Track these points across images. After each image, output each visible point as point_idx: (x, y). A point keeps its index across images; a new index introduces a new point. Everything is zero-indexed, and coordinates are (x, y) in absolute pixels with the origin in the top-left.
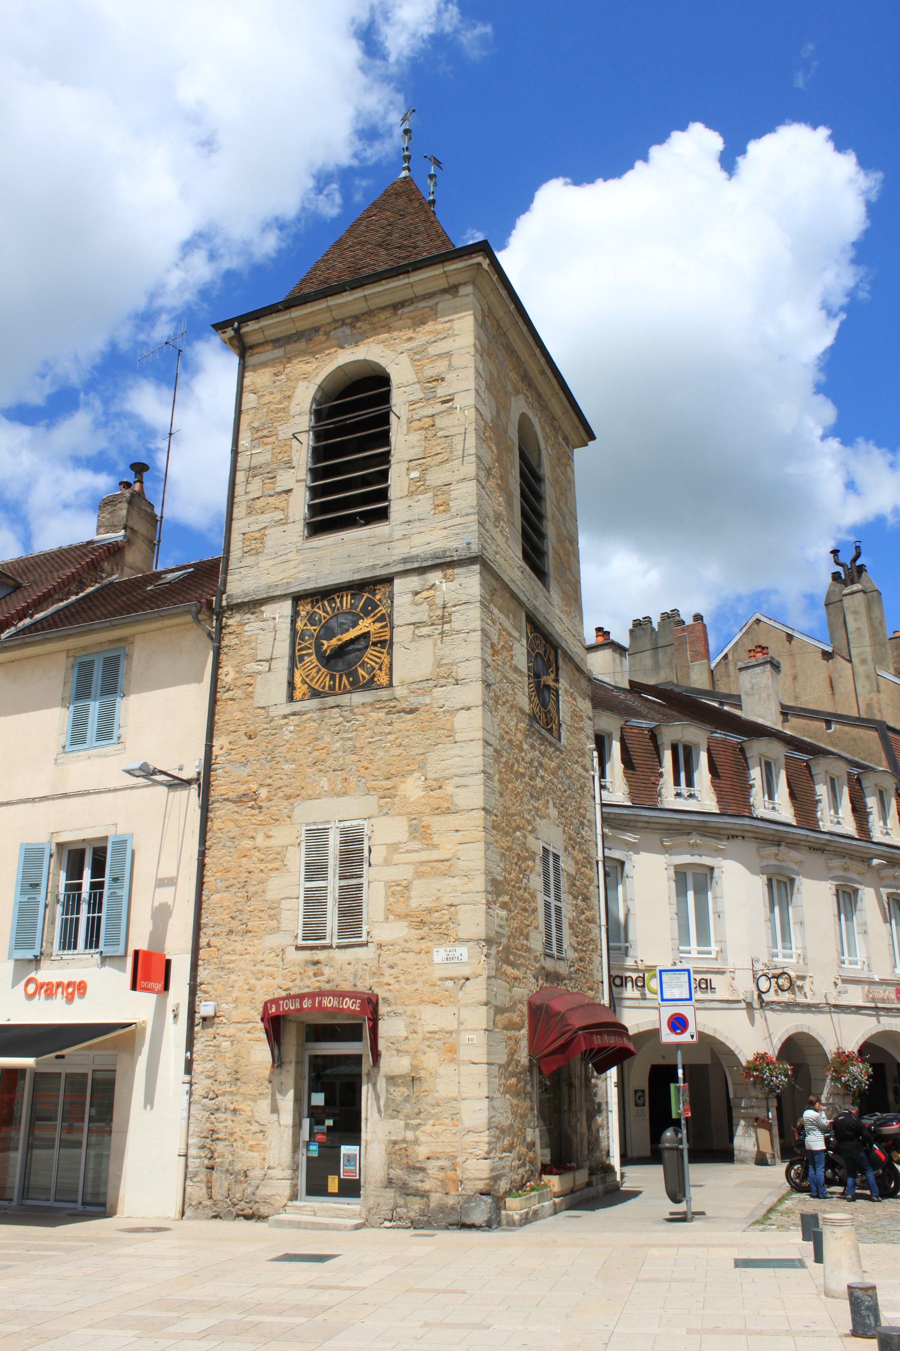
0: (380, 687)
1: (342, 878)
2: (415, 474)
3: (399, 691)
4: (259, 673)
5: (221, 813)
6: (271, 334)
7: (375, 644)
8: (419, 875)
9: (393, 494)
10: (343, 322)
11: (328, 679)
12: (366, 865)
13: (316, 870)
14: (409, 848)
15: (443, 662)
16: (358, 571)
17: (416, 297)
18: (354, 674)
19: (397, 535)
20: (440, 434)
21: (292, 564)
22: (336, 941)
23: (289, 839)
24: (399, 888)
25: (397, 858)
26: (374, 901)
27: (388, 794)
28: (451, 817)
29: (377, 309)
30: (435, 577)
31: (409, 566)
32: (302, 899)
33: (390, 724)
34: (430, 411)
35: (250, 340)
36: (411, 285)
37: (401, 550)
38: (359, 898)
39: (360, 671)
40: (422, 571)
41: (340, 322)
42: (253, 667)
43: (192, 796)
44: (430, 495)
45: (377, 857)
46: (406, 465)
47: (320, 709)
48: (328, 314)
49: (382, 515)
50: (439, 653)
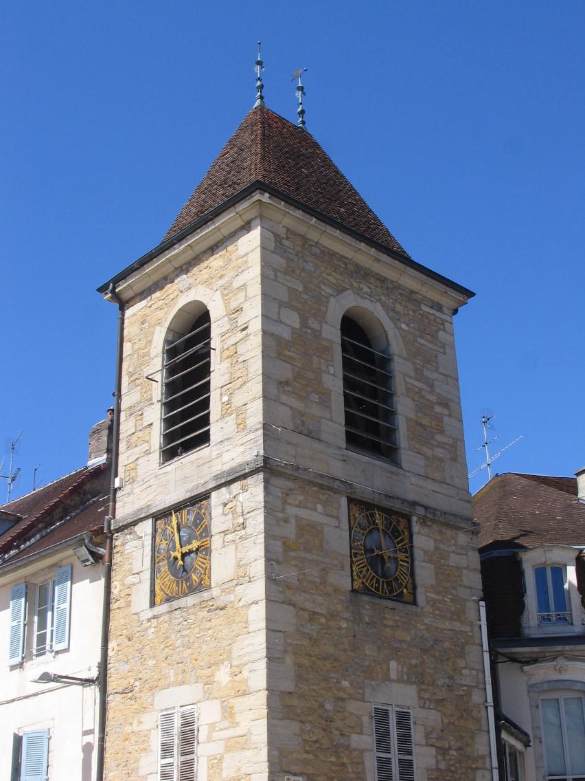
2: (225, 399)
3: (215, 592)
4: (134, 584)
5: (113, 701)
6: (138, 288)
8: (228, 749)
9: (212, 418)
11: (175, 585)
13: (166, 750)
14: (222, 727)
15: (241, 564)
17: (225, 237)
18: (189, 579)
19: (214, 455)
20: (240, 360)
23: (151, 721)
24: (216, 761)
27: (209, 682)
28: (246, 698)
29: (201, 253)
33: (210, 621)
35: (125, 296)
36: (218, 229)
38: (191, 771)
40: (229, 483)
41: (179, 269)
42: (130, 580)
43: (93, 692)
44: (234, 416)
45: (202, 736)
47: (169, 612)
48: (169, 265)
50: (239, 555)
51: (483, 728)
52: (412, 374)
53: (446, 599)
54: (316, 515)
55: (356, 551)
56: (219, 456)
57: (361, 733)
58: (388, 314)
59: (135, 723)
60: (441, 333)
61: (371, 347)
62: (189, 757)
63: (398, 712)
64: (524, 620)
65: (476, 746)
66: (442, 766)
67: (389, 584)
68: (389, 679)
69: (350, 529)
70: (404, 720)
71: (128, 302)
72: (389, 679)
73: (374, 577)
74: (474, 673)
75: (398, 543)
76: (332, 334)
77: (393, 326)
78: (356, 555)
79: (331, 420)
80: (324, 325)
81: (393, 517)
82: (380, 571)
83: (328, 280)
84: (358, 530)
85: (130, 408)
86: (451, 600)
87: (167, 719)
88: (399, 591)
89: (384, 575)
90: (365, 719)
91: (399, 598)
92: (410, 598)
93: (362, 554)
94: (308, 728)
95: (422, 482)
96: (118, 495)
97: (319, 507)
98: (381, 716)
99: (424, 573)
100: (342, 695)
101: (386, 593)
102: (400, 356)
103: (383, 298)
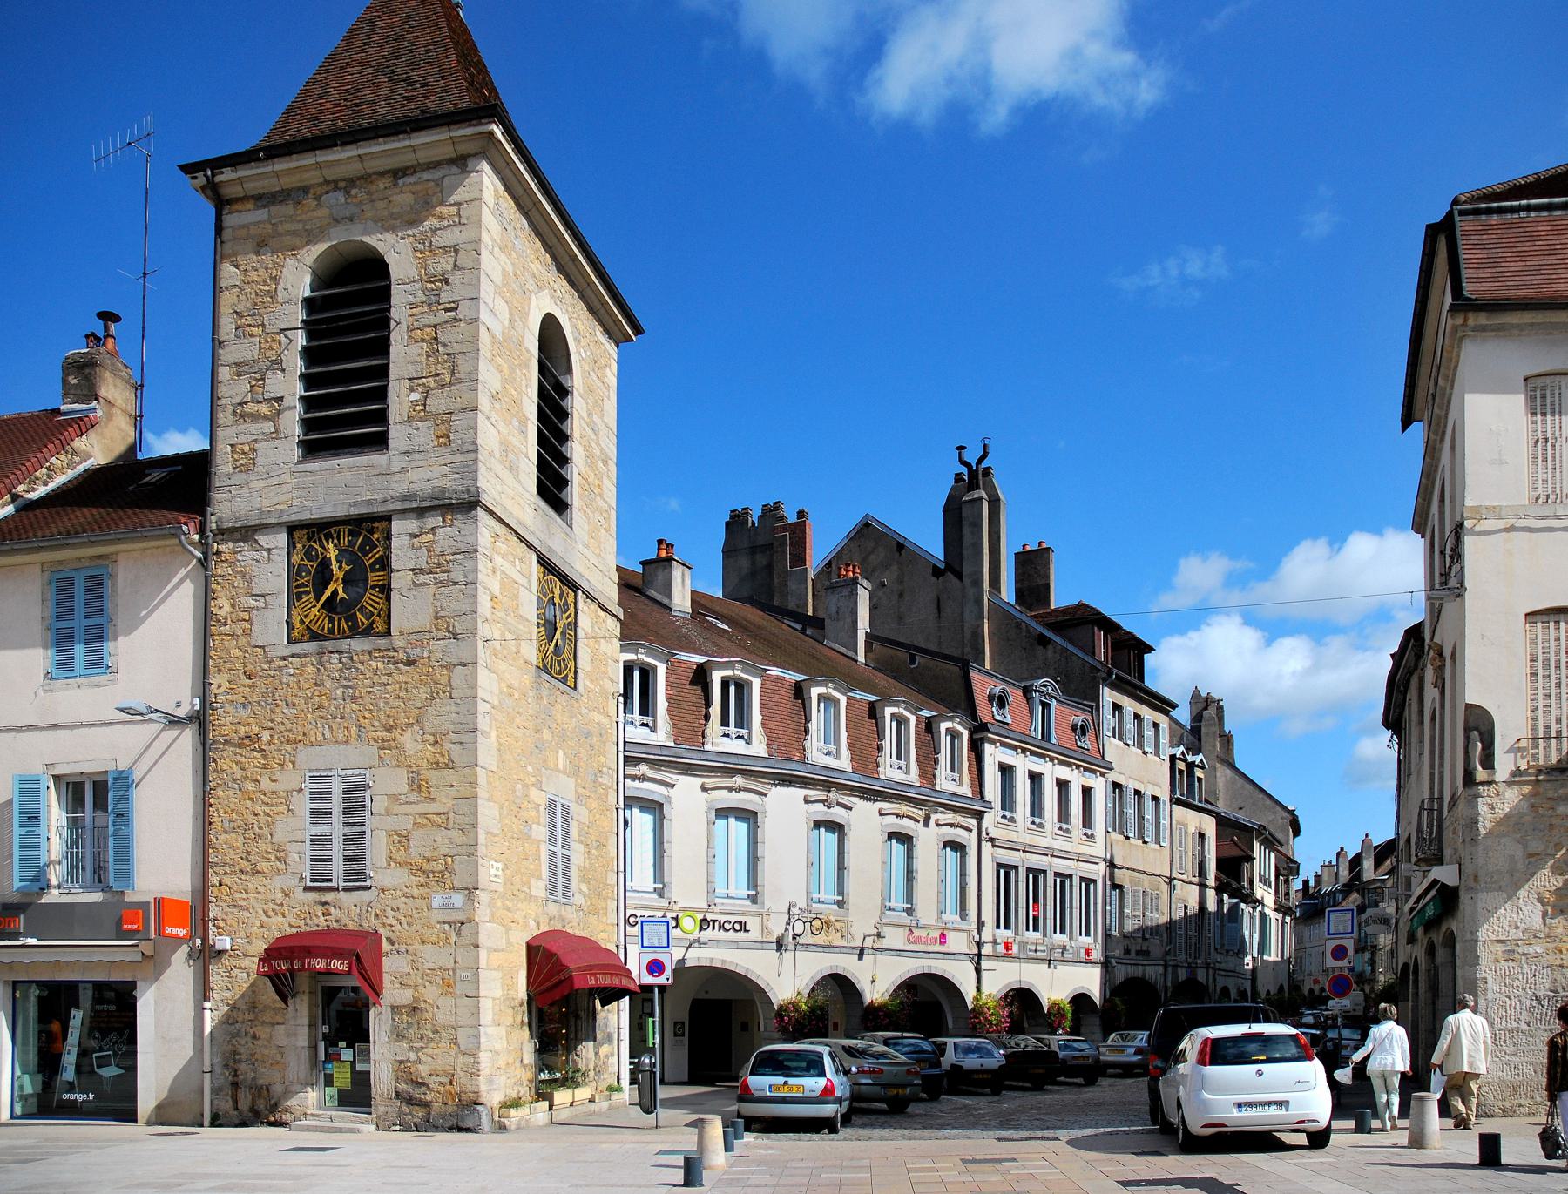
0: (378, 635)
1: (346, 825)
2: (415, 396)
3: (398, 641)
6: (252, 187)
7: (373, 588)
9: (393, 416)
10: (334, 185)
12: (368, 815)
16: (355, 504)
18: (353, 618)
19: (396, 467)
21: (285, 488)
22: (342, 885)
25: (397, 809)
26: (377, 848)
30: (434, 521)
31: (407, 505)
32: (308, 843)
34: (432, 320)
37: (400, 485)
38: (361, 846)
39: (359, 616)
43: (188, 736)
45: (380, 804)
46: (407, 383)
49: (379, 442)
50: (438, 604)
56: (404, 470)
62: (357, 829)
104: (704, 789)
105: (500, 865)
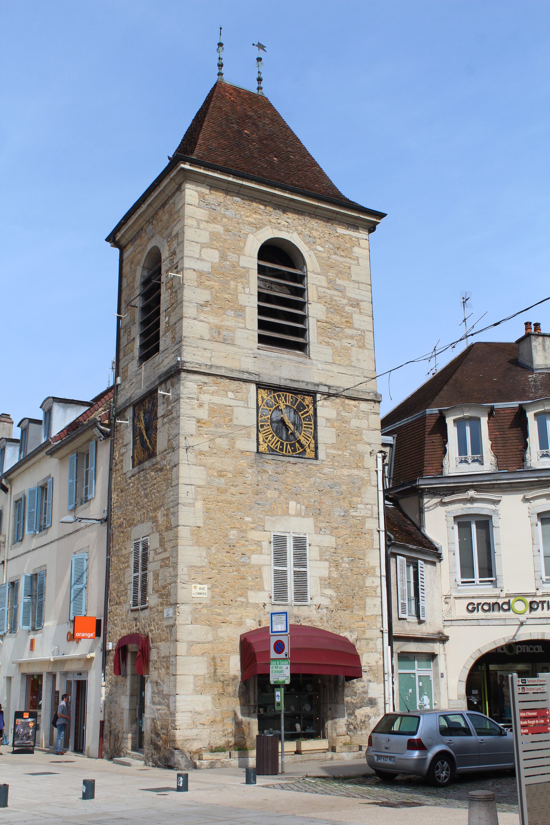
3: (158, 458)
8: (162, 567)
27: (154, 520)
42: (123, 450)
51: (374, 546)
52: (325, 284)
53: (345, 453)
54: (229, 399)
55: (262, 423)
57: (261, 553)
58: (303, 241)
59: (123, 549)
60: (356, 249)
61: (294, 267)
63: (295, 538)
64: (445, 462)
65: (367, 560)
66: (335, 575)
67: (291, 445)
68: (288, 514)
69: (258, 408)
70: (300, 544)
71: (125, 247)
72: (288, 514)
73: (278, 441)
74: (369, 507)
75: (302, 415)
76: (251, 261)
77: (308, 249)
78: (262, 426)
79: (245, 328)
80: (241, 256)
81: (299, 396)
82: (284, 436)
83: (247, 221)
84: (266, 407)
85: (125, 326)
86: (350, 454)
87: (137, 545)
88: (301, 450)
89: (288, 439)
90: (265, 544)
91: (302, 455)
92: (313, 455)
93: (268, 425)
94: (214, 551)
95: (329, 367)
96: (119, 390)
97: (230, 394)
98: (279, 542)
99: (326, 435)
100: (244, 527)
101: (289, 452)
102: (313, 272)
103: (300, 228)
104: (526, 500)
105: (206, 586)
